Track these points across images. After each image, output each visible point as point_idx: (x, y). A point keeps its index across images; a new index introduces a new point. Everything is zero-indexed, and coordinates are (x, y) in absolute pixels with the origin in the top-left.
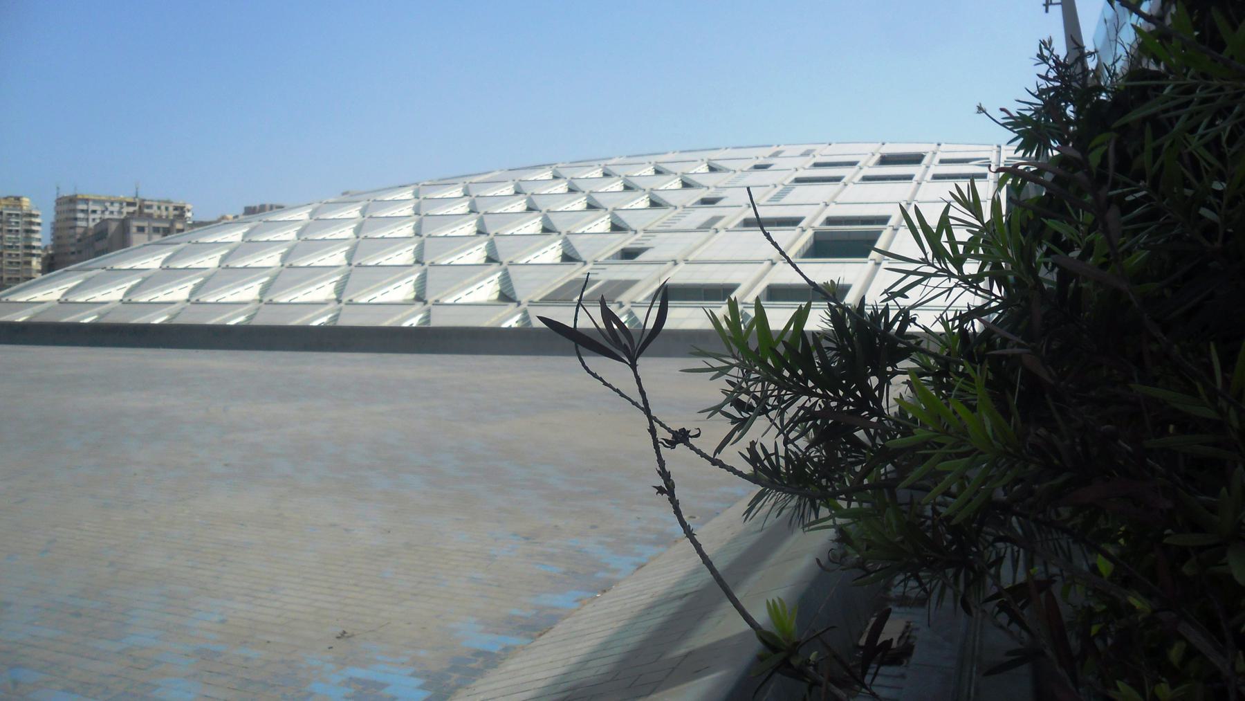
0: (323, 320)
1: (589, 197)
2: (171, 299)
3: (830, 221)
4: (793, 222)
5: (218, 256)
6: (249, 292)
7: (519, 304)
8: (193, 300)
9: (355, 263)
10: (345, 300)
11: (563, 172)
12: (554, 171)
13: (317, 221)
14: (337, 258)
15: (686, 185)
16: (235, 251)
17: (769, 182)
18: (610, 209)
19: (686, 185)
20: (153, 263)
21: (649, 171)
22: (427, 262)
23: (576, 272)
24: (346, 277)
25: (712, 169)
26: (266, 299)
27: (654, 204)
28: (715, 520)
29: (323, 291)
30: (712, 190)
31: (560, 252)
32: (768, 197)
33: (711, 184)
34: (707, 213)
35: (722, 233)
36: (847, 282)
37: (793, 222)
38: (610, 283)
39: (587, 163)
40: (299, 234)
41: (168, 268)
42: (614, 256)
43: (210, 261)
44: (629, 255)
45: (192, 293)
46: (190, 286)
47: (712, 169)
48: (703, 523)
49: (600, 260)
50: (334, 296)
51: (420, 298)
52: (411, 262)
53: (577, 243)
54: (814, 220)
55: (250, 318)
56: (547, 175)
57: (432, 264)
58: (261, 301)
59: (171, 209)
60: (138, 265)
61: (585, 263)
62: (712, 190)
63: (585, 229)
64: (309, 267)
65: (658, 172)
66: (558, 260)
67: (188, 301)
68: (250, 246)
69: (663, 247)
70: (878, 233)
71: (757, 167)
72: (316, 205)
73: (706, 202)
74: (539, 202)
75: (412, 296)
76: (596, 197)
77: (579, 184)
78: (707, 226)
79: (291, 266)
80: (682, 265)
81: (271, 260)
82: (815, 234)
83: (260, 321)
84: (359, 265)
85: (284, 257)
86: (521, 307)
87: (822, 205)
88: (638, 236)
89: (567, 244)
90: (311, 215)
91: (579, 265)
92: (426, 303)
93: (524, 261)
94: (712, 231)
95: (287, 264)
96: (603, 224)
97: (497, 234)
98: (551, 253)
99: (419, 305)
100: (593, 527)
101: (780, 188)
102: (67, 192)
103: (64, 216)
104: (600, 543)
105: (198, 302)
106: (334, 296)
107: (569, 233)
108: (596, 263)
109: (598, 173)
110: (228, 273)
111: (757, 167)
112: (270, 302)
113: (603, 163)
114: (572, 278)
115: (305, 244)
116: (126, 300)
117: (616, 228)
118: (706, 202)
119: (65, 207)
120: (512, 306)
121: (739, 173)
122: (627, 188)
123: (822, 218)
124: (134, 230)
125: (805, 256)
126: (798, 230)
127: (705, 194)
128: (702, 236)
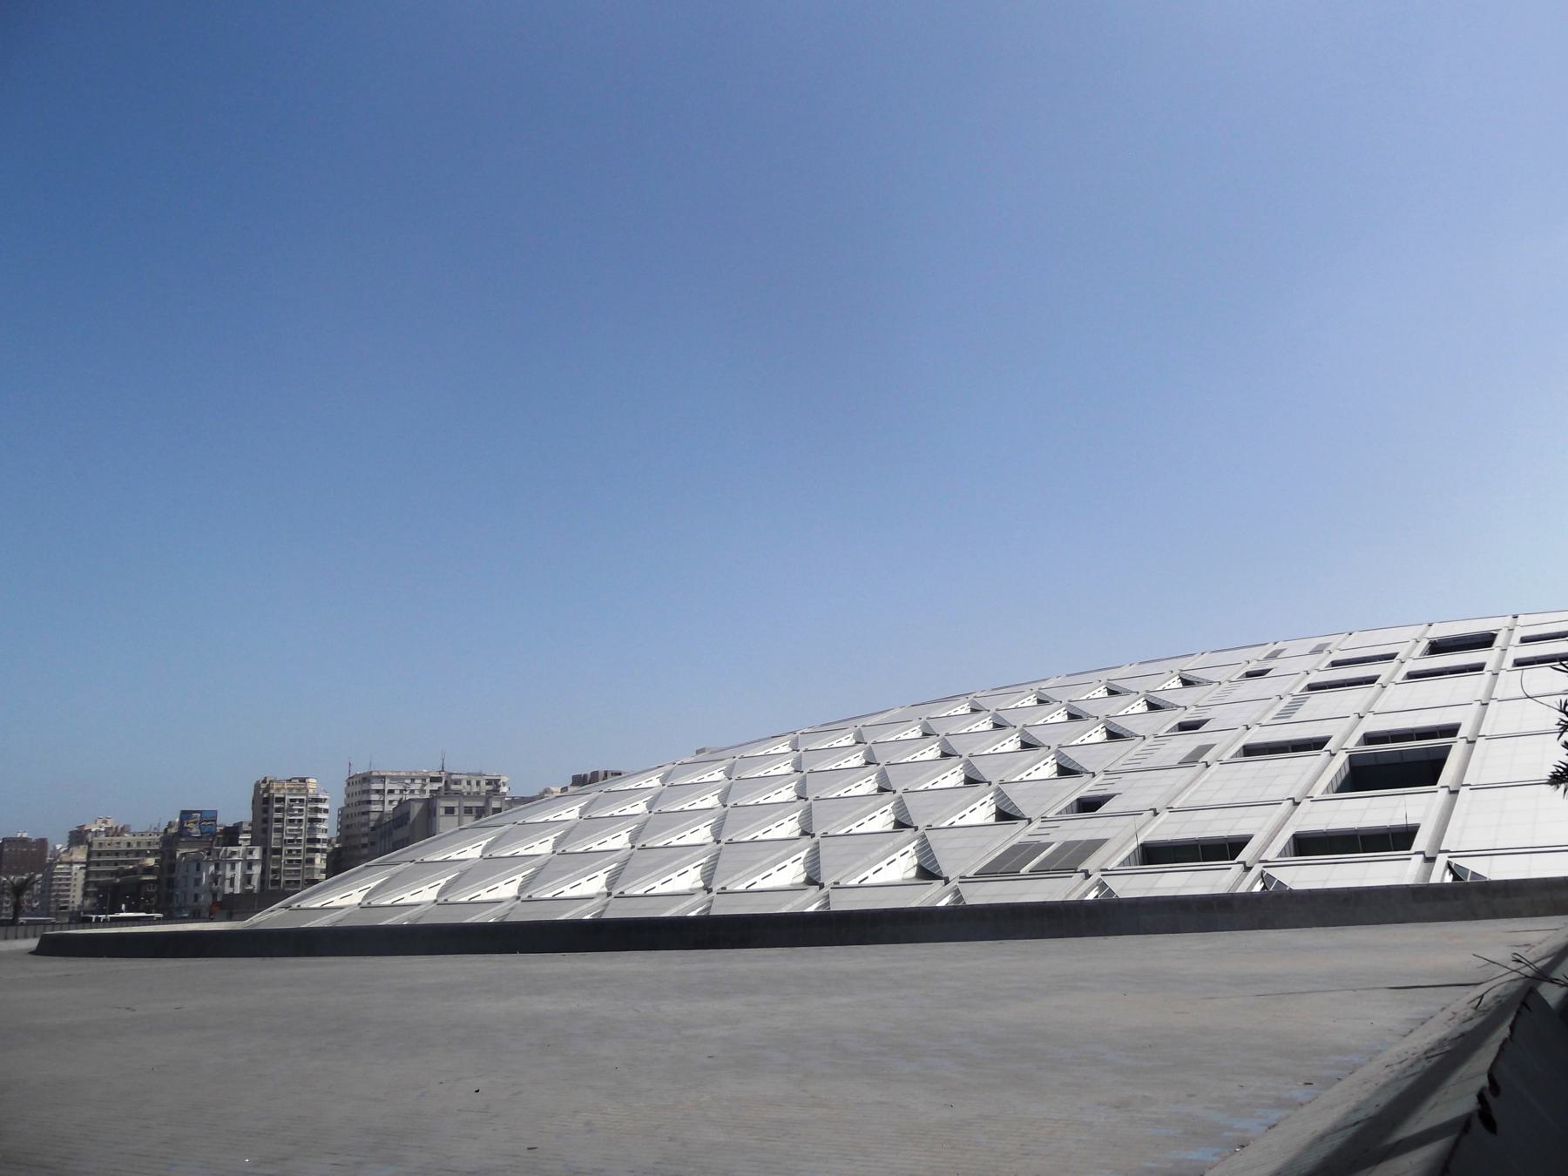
1: (1023, 732)
2: (500, 895)
3: (1369, 739)
4: (1317, 744)
5: (551, 839)
6: (593, 884)
7: (947, 881)
8: (524, 896)
9: (724, 840)
10: (716, 888)
12: (973, 702)
13: (671, 787)
14: (701, 834)
15: (1153, 707)
16: (570, 832)
17: (1272, 692)
18: (1054, 747)
19: (1153, 707)
20: (473, 852)
21: (1101, 692)
22: (818, 834)
23: (1017, 834)
25: (1187, 683)
26: (615, 892)
27: (1113, 735)
29: (688, 879)
31: (993, 809)
33: (1190, 703)
34: (1191, 741)
35: (1215, 767)
36: (1410, 822)
37: (1317, 744)
38: (1067, 846)
39: (1014, 688)
40: (650, 806)
41: (490, 857)
42: (1068, 810)
44: (1088, 805)
45: (522, 889)
46: (519, 879)
47: (1187, 683)
49: (1050, 815)
50: (701, 884)
51: (812, 881)
52: (796, 834)
53: (1013, 793)
54: (1346, 741)
56: (964, 709)
57: (825, 836)
58: (609, 894)
59: (483, 783)
60: (454, 856)
61: (1030, 821)
63: (1023, 776)
65: (1112, 693)
66: (992, 820)
68: (590, 824)
69: (1133, 793)
70: (1447, 749)
71: (1249, 675)
72: (668, 768)
73: (1184, 727)
74: (955, 744)
75: (802, 879)
76: (1034, 732)
77: (1007, 717)
78: (1193, 759)
79: (644, 848)
80: (1164, 816)
81: (619, 841)
84: (730, 842)
85: (633, 838)
86: (950, 886)
87: (1354, 717)
88: (1097, 780)
89: (1000, 796)
90: (663, 780)
91: (1022, 823)
92: (822, 886)
93: (945, 824)
94: (1200, 766)
95: (639, 845)
96: (1047, 769)
97: (906, 791)
98: (983, 812)
99: (813, 889)
101: (1288, 699)
102: (360, 769)
103: (355, 799)
105: (530, 900)
107: (1002, 782)
108: (1044, 819)
109: (1031, 701)
110: (566, 860)
111: (1249, 675)
112: (622, 896)
113: (1036, 687)
114: (1015, 842)
115: (659, 816)
116: (441, 900)
117: (1064, 771)
118: (1184, 727)
119: (358, 788)
120: (938, 884)
122: (1072, 717)
123: (1358, 735)
124: (441, 811)
125: (1339, 790)
126: (1323, 755)
128: (1188, 773)
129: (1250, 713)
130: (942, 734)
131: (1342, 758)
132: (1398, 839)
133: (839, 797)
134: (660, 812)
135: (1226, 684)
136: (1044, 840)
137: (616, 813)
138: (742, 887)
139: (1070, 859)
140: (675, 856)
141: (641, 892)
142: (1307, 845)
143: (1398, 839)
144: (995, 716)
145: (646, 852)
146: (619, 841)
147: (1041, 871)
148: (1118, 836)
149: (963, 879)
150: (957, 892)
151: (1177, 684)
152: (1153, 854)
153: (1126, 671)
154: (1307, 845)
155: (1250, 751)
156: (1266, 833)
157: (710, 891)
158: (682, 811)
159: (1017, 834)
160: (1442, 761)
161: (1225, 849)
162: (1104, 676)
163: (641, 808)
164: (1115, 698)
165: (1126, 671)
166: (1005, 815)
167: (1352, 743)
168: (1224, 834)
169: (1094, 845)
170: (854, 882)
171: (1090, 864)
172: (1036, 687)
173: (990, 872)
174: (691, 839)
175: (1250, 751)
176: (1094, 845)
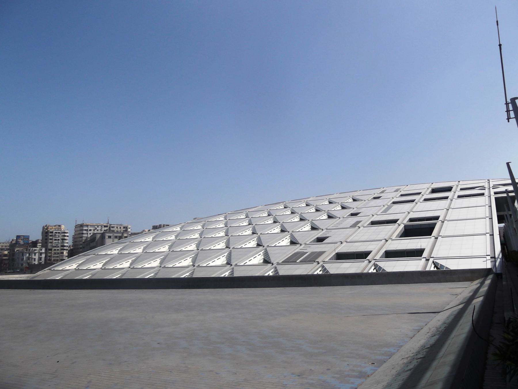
0: (186, 275)
1: (301, 215)
3: (411, 220)
4: (394, 221)
5: (142, 247)
6: (155, 263)
7: (273, 264)
8: (132, 267)
10: (196, 265)
11: (288, 205)
13: (184, 231)
14: (192, 247)
15: (343, 208)
16: (149, 245)
18: (310, 220)
19: (343, 208)
20: (115, 252)
22: (231, 247)
23: (297, 249)
24: (197, 255)
25: (354, 200)
26: (162, 266)
27: (330, 217)
28: (385, 365)
29: (187, 262)
30: (355, 209)
32: (381, 211)
33: (355, 207)
34: (355, 219)
35: (362, 228)
37: (394, 221)
38: (312, 253)
39: (298, 200)
40: (176, 237)
41: (121, 254)
42: (313, 241)
43: (139, 250)
44: (320, 240)
45: (131, 264)
46: (130, 261)
47: (354, 200)
48: (379, 367)
50: (191, 264)
51: (229, 263)
52: (224, 247)
53: (296, 235)
54: (404, 221)
55: (156, 274)
57: (234, 248)
58: (160, 267)
59: (122, 228)
60: (109, 253)
61: (301, 245)
62: (355, 209)
63: (300, 230)
64: (180, 251)
65: (330, 203)
66: (289, 244)
67: (129, 267)
68: (155, 243)
69: (335, 236)
70: (435, 224)
71: (375, 198)
73: (353, 215)
74: (278, 218)
75: (225, 262)
76: (304, 215)
77: (296, 210)
78: (354, 225)
79: (173, 251)
80: (344, 244)
82: (405, 226)
83: (159, 276)
84: (202, 250)
85: (170, 248)
88: (324, 231)
89: (292, 236)
90: (181, 228)
91: (298, 245)
92: (231, 265)
93: (273, 245)
94: (357, 228)
95: (171, 250)
96: (308, 228)
98: (286, 241)
100: (328, 369)
101: (386, 206)
104: (333, 377)
105: (133, 268)
106: (191, 264)
107: (293, 232)
108: (305, 244)
109: (304, 205)
110: (147, 255)
111: (375, 198)
112: (165, 267)
113: (306, 200)
114: (296, 251)
115: (179, 241)
116: (103, 268)
117: (313, 228)
118: (353, 215)
120: (269, 265)
121: (367, 201)
122: (317, 210)
124: (107, 237)
125: (400, 237)
126: (396, 225)
127: (353, 211)
128: (353, 230)
129: (374, 210)
130: (274, 215)
131: (402, 226)
132: (418, 253)
133: (239, 235)
134: (179, 239)
135: (367, 201)
136: (305, 251)
137: (165, 239)
138: (205, 265)
139: (313, 258)
140: (184, 254)
141: (171, 266)
142: (390, 255)
143: (418, 253)
144: (292, 209)
145: (174, 253)
146: (165, 249)
147: (304, 262)
148: (329, 250)
149: (278, 264)
150: (276, 268)
151: (351, 200)
152: (340, 257)
153: (335, 196)
154: (390, 255)
155: (373, 223)
156: (377, 250)
157: (194, 266)
158: (187, 239)
159: (297, 249)
160: (434, 228)
161: (363, 255)
162: (328, 197)
163: (173, 237)
164: (331, 205)
165: (335, 196)
166: (293, 243)
167: (405, 222)
168: (363, 250)
169: (321, 253)
170: (242, 264)
171: (320, 259)
172: (306, 200)
173: (287, 262)
174: (189, 248)
175: (373, 223)
176: (321, 253)
